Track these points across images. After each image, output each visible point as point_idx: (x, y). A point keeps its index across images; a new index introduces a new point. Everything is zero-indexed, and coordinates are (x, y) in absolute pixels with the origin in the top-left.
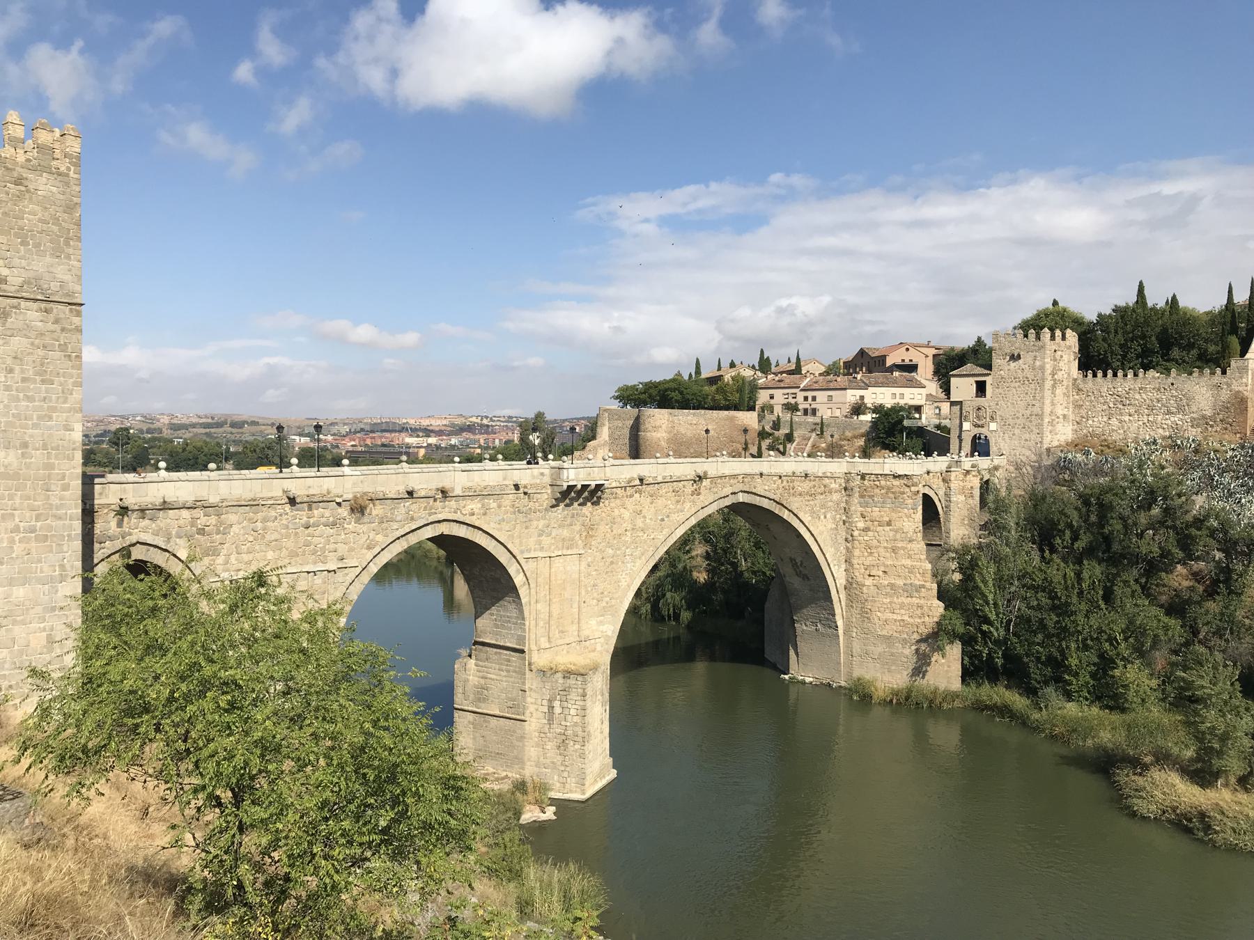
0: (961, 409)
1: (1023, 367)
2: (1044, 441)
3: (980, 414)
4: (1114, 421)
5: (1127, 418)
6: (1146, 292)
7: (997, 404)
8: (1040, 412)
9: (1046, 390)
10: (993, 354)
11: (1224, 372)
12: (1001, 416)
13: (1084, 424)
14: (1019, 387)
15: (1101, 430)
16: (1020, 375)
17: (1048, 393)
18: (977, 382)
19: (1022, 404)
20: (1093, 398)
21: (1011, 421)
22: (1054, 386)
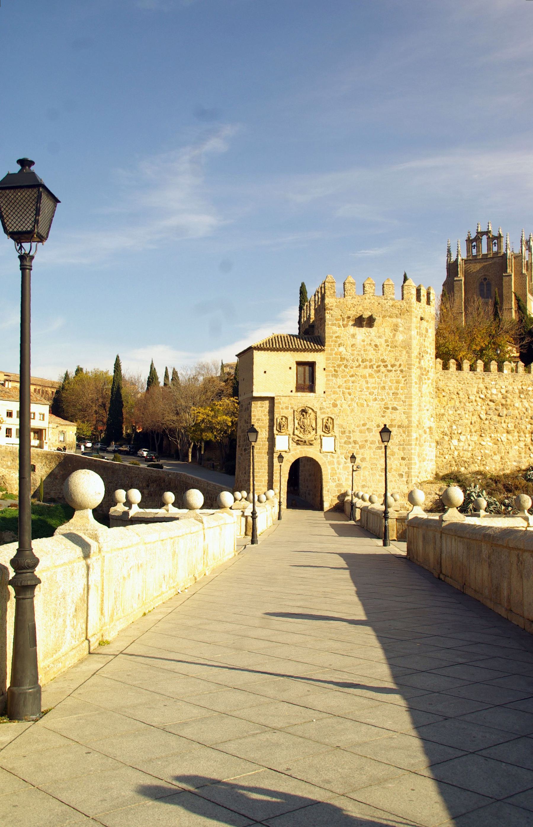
0: (271, 412)
1: (377, 341)
2: (414, 472)
4: (487, 442)
5: (504, 437)
6: (403, 280)
7: (335, 405)
8: (406, 423)
9: (413, 384)
10: (328, 316)
12: (341, 426)
13: (446, 446)
14: (371, 375)
15: (469, 454)
16: (371, 354)
17: (415, 389)
18: (299, 364)
19: (376, 406)
20: (458, 404)
21: (357, 436)
22: (420, 379)
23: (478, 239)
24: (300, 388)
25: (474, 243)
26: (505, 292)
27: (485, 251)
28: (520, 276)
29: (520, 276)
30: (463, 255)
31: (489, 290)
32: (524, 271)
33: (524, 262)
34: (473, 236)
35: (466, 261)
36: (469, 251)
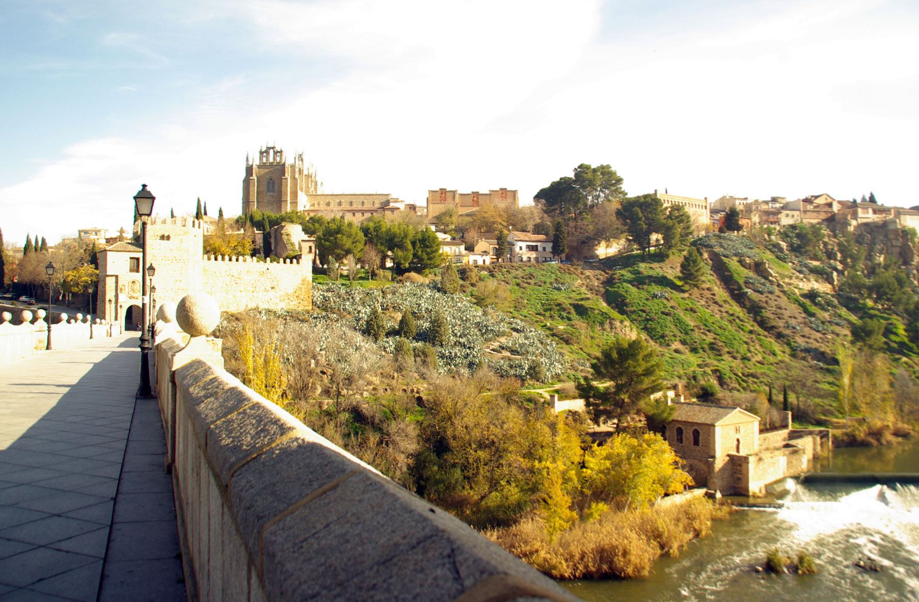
0: (117, 282)
3: (135, 287)
11: (298, 263)
18: (131, 258)
23: (267, 152)
24: (131, 270)
25: (265, 154)
26: (283, 189)
27: (271, 160)
28: (294, 178)
29: (294, 178)
30: (257, 162)
31: (273, 187)
32: (297, 176)
33: (297, 170)
34: (264, 149)
35: (259, 167)
36: (261, 159)
